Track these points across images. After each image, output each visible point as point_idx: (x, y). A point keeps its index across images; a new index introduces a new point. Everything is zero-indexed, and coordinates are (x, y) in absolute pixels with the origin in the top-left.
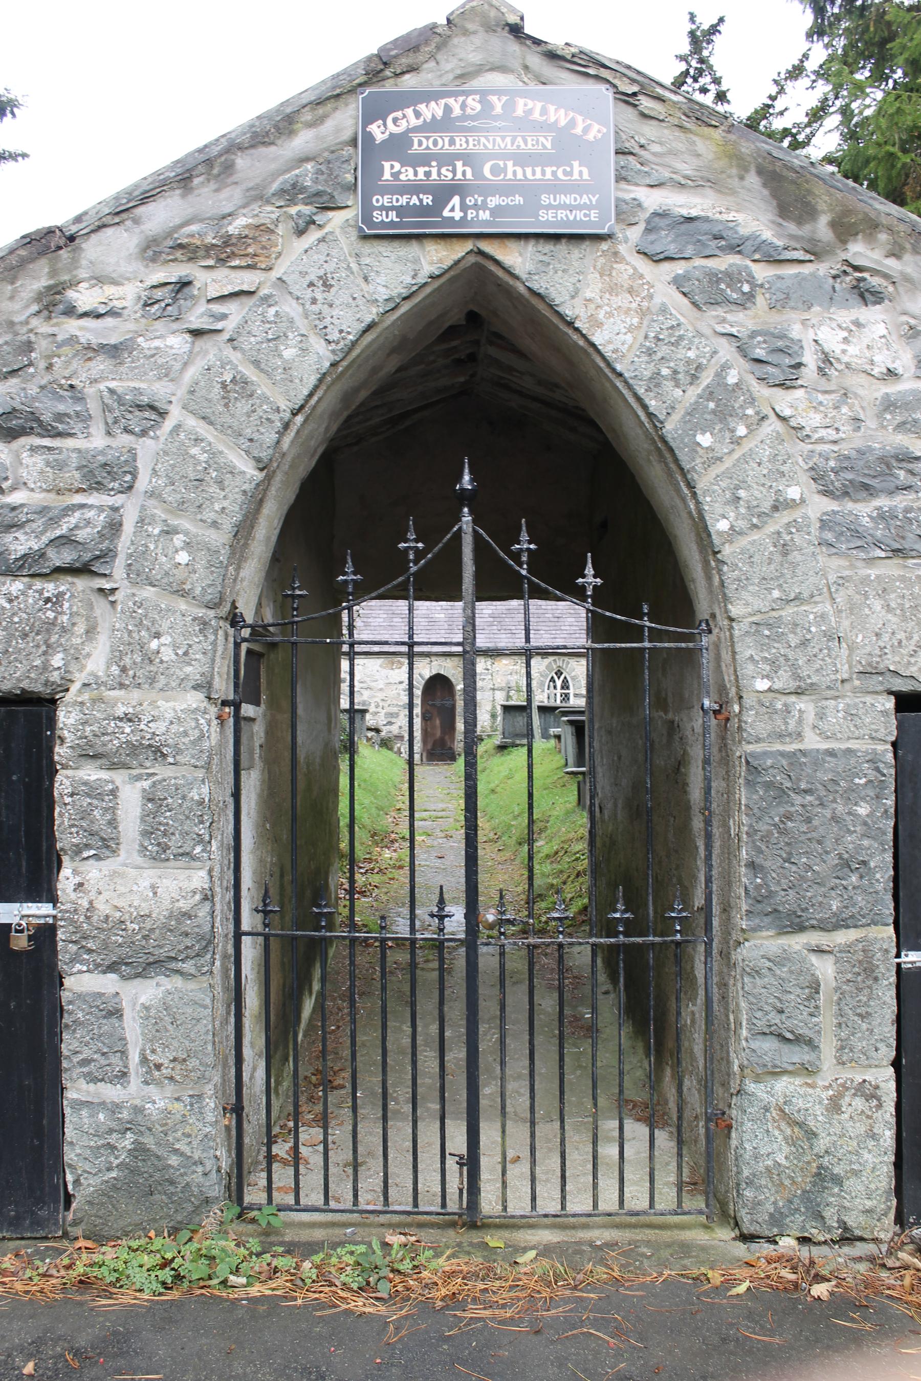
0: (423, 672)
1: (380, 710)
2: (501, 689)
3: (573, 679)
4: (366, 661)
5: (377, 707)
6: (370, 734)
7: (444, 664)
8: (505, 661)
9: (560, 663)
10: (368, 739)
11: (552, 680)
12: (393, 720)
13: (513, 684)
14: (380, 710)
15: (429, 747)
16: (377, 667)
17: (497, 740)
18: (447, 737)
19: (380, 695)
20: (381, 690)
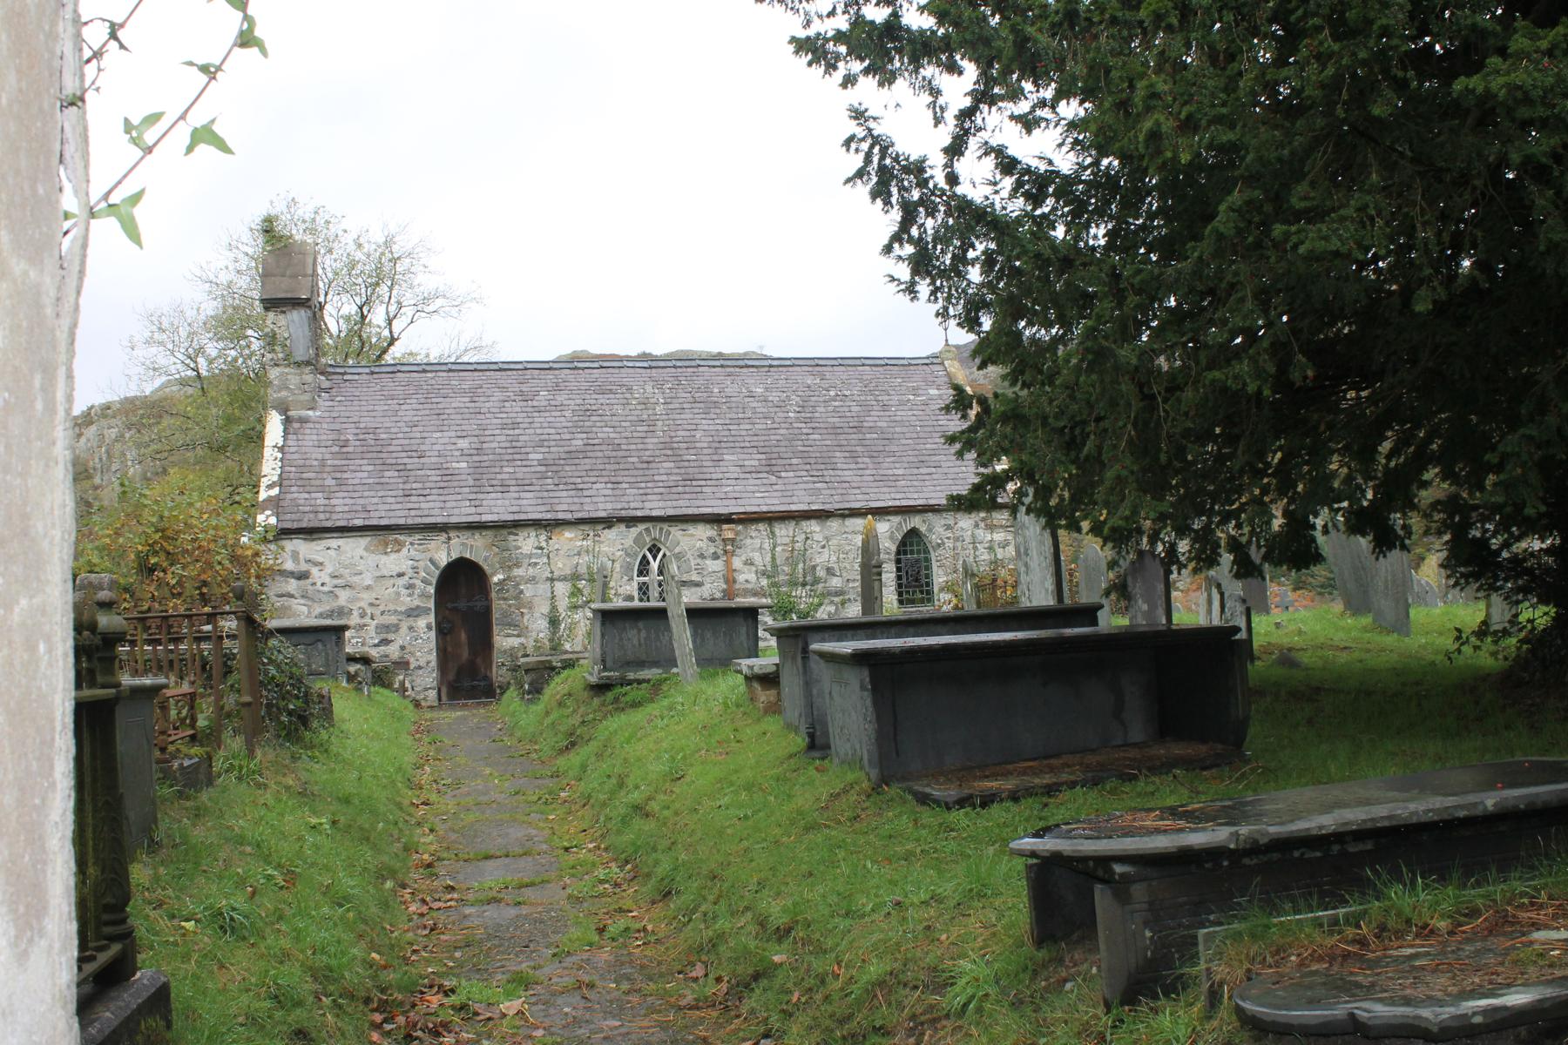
0: (436, 557)
1: (367, 620)
2: (564, 579)
3: (679, 557)
4: (340, 542)
5: (362, 616)
6: (353, 668)
7: (470, 542)
8: (568, 534)
9: (655, 533)
10: (351, 678)
12: (391, 636)
13: (583, 570)
14: (367, 620)
15: (451, 677)
16: (361, 551)
17: (589, 672)
18: (479, 661)
19: (367, 597)
20: (368, 588)
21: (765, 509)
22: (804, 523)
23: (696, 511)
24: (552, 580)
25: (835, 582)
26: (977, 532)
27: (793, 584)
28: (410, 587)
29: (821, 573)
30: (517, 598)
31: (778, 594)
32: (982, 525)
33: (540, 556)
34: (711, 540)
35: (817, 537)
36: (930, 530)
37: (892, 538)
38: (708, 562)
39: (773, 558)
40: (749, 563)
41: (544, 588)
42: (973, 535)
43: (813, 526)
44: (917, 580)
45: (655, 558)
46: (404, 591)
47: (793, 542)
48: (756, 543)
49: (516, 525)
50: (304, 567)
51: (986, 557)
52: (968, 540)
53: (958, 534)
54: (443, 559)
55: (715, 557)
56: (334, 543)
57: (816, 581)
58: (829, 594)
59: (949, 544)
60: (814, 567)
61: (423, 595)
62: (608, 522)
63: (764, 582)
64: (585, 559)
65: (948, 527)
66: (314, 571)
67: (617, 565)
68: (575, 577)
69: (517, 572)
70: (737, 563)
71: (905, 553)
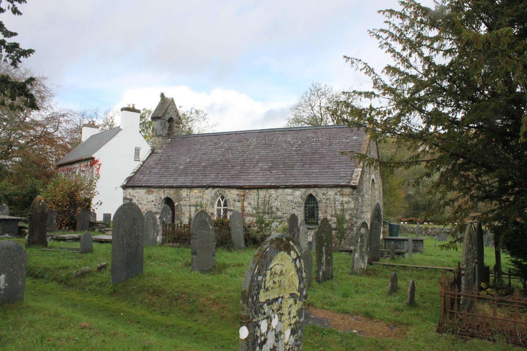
2: (193, 206)
8: (196, 191)
11: (219, 201)
13: (199, 203)
20: (145, 205)
21: (256, 184)
22: (270, 190)
23: (233, 184)
24: (190, 206)
25: (279, 214)
26: (336, 196)
27: (264, 213)
28: (155, 205)
29: (274, 210)
30: (181, 211)
31: (259, 216)
32: (338, 194)
33: (187, 198)
34: (238, 195)
35: (274, 196)
36: (317, 195)
37: (301, 197)
38: (237, 203)
39: (258, 203)
40: (250, 204)
41: (188, 208)
42: (334, 198)
43: (272, 191)
44: (313, 215)
45: (222, 200)
46: (154, 207)
47: (265, 197)
48: (253, 196)
49: (181, 187)
50: (131, 197)
51: (340, 207)
52: (332, 200)
53: (328, 197)
54: (163, 197)
55: (239, 201)
56: (138, 190)
57: (272, 213)
58: (277, 218)
59: (324, 201)
60: (272, 207)
61: (158, 208)
62: (207, 187)
63: (255, 212)
64: (199, 200)
65: (324, 194)
66: (134, 198)
67: (209, 202)
68: (196, 205)
69: (181, 203)
70: (245, 204)
71: (309, 204)
